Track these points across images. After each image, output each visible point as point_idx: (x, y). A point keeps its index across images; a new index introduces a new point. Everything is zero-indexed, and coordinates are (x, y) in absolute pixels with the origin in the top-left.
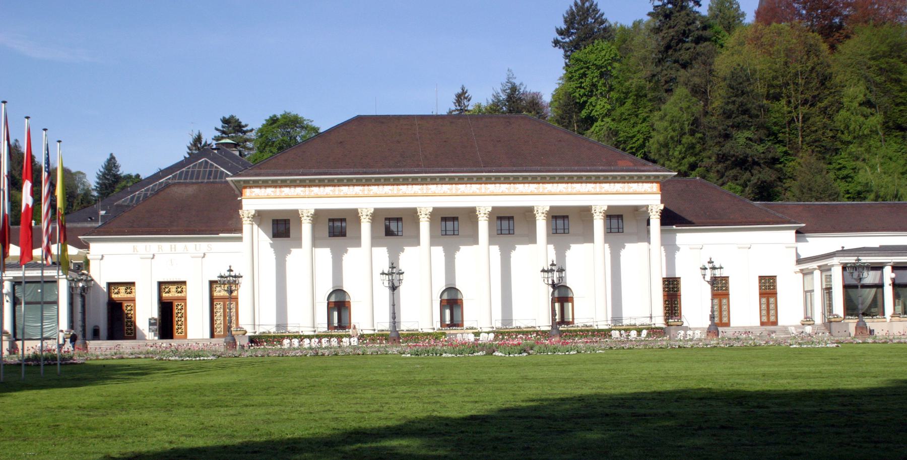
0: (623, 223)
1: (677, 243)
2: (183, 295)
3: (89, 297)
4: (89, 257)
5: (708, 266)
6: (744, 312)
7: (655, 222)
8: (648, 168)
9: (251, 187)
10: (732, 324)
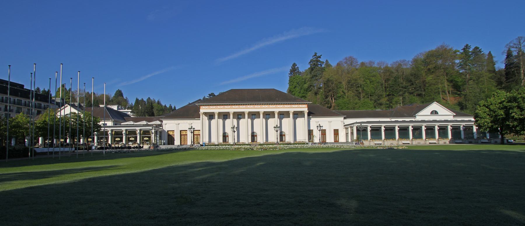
0: (297, 115)
6: (330, 138)
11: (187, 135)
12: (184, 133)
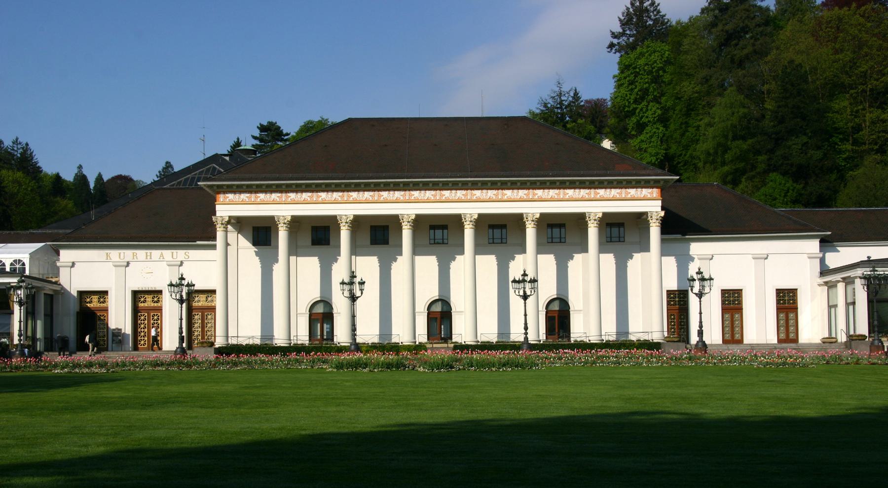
0: (621, 232)
1: (691, 253)
2: (159, 305)
3: (58, 309)
4: (58, 264)
5: (695, 277)
6: (760, 327)
7: (655, 231)
8: (648, 172)
9: (224, 193)
10: (745, 342)
11: (160, 309)
12: (149, 302)
